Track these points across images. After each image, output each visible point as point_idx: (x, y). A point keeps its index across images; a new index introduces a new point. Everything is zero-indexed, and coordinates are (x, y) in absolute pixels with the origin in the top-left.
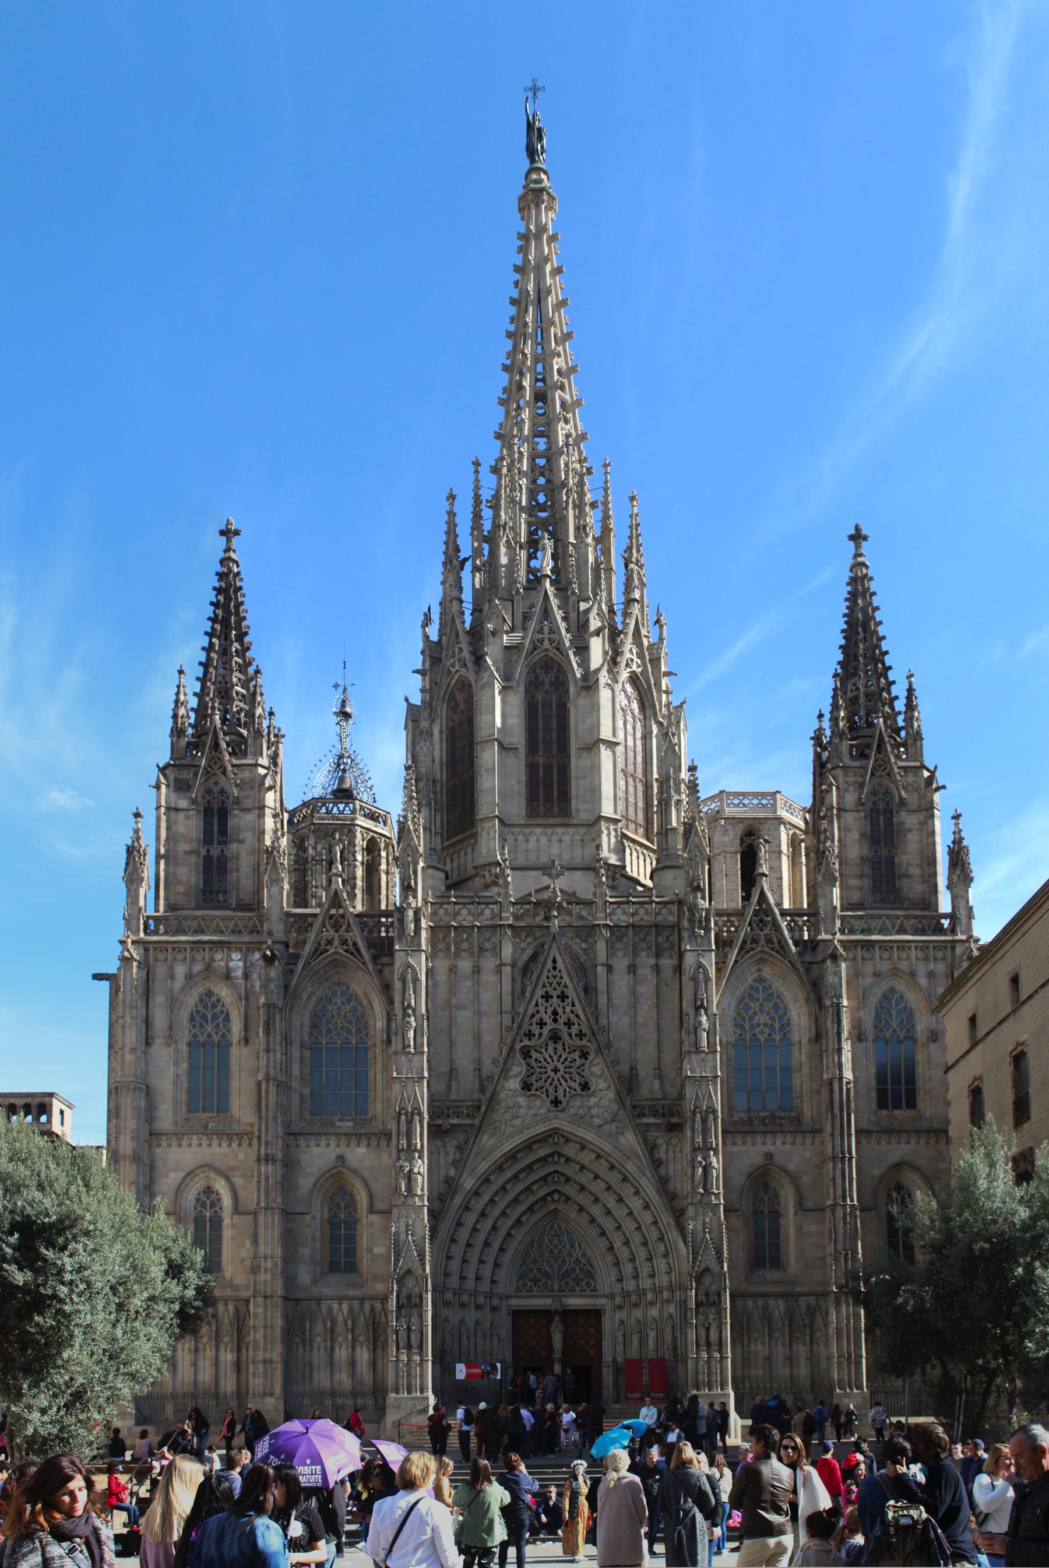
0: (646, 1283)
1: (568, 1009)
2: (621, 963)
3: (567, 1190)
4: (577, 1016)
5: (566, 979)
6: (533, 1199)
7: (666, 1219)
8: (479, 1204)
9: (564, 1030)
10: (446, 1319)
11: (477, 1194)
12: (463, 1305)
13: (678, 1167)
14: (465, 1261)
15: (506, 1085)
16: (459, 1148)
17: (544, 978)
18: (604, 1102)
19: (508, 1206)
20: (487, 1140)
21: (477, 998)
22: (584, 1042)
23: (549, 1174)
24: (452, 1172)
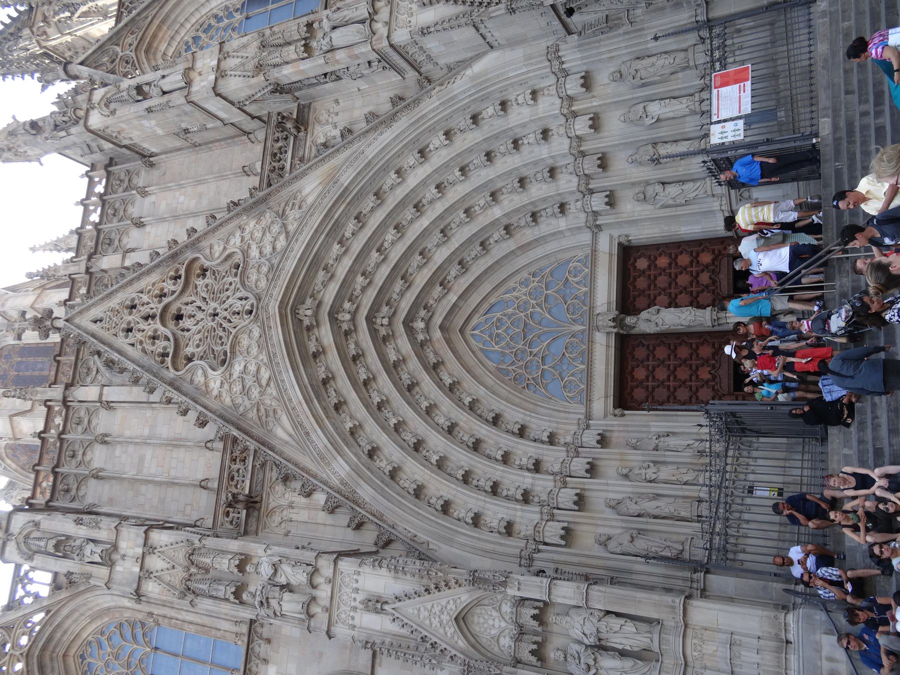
0: (560, 145)
1: (145, 298)
2: (134, 238)
3: (405, 306)
4: (154, 285)
5: (114, 302)
6: (414, 364)
7: (430, 105)
8: (392, 452)
9: (166, 300)
10: (604, 542)
11: (372, 453)
12: (581, 502)
13: (359, 103)
14: (495, 490)
15: (215, 393)
16: (286, 479)
17: (106, 335)
18: (258, 235)
19: (414, 405)
20: (282, 432)
21: (130, 442)
22: (182, 272)
23: (373, 332)
24: (320, 498)
